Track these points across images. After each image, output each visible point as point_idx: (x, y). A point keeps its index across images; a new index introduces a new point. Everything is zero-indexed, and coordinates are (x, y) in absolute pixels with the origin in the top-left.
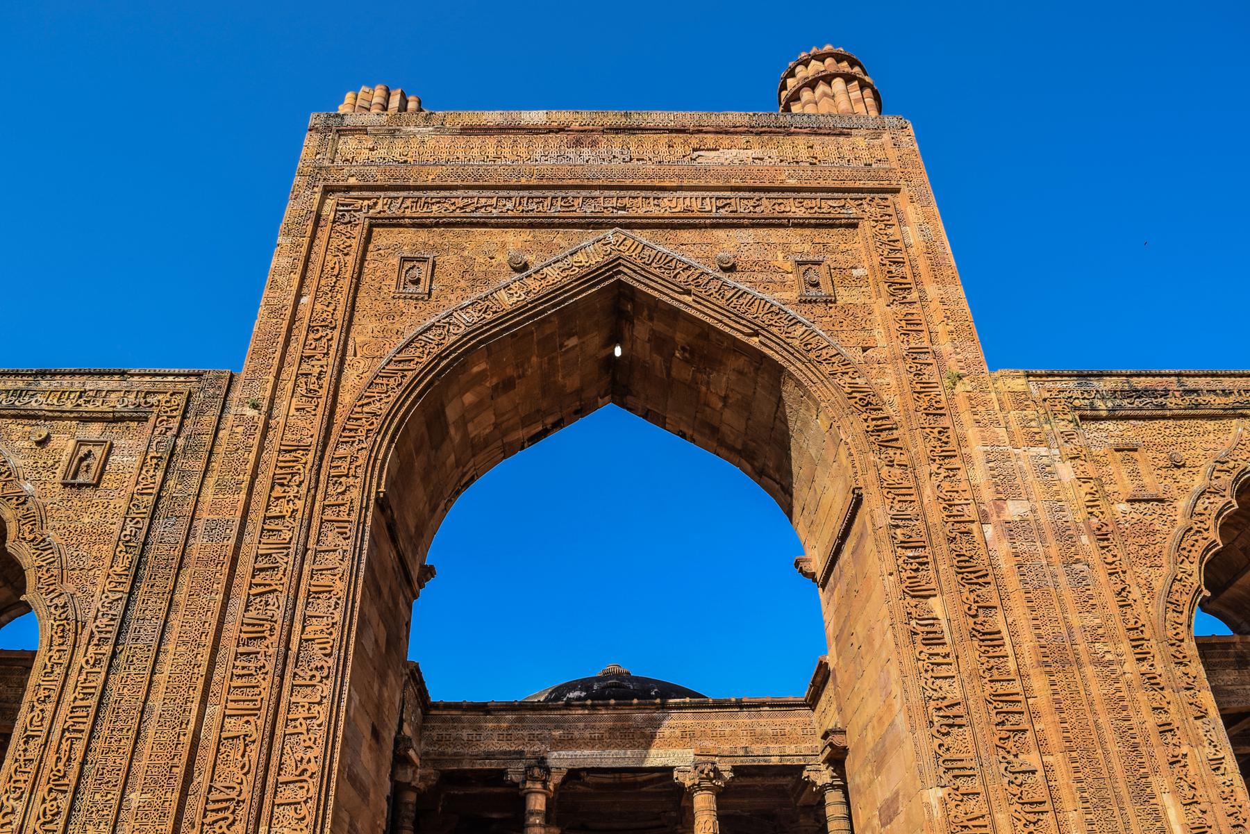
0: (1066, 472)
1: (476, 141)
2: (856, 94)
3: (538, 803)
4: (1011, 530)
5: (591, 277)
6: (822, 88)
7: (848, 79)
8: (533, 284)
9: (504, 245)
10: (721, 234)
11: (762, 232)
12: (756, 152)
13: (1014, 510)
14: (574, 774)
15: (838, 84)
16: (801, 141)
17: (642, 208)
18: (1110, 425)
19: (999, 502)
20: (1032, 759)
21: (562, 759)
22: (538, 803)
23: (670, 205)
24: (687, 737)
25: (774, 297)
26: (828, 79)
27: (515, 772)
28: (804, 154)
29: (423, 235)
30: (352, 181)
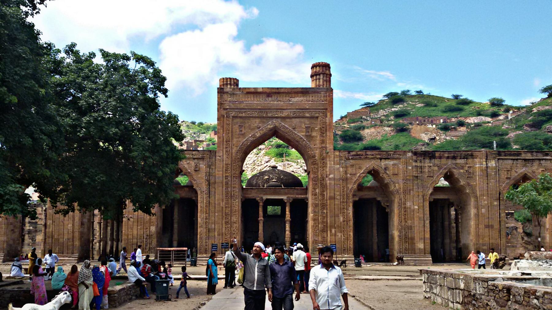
0: (341, 169)
1: (249, 96)
2: (325, 78)
3: (261, 204)
4: (330, 179)
5: (271, 130)
6: (318, 77)
7: (323, 74)
8: (262, 132)
9: (256, 122)
10: (293, 120)
11: (301, 119)
12: (302, 98)
13: (331, 176)
14: (267, 199)
15: (321, 76)
16: (311, 95)
17: (280, 115)
18: (351, 161)
19: (329, 175)
20: (325, 211)
21: (265, 197)
22: (261, 204)
23: (285, 114)
24: (285, 194)
25: (302, 135)
26: (319, 75)
27: (258, 199)
28: (311, 99)
29: (242, 120)
30: (228, 107)
